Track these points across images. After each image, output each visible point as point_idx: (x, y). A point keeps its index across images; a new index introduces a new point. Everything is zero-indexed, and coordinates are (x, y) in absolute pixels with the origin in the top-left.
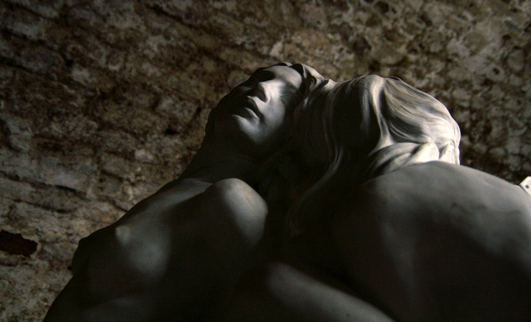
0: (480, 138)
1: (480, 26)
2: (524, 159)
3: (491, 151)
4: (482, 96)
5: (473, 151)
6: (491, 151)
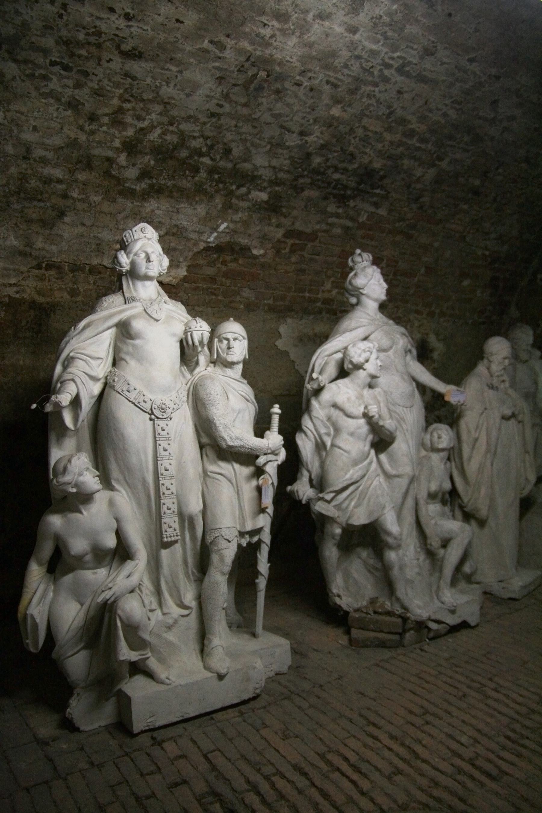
0: (221, 158)
1: (187, 74)
2: (277, 170)
3: (238, 166)
4: (210, 126)
5: (219, 168)
6: (238, 166)
